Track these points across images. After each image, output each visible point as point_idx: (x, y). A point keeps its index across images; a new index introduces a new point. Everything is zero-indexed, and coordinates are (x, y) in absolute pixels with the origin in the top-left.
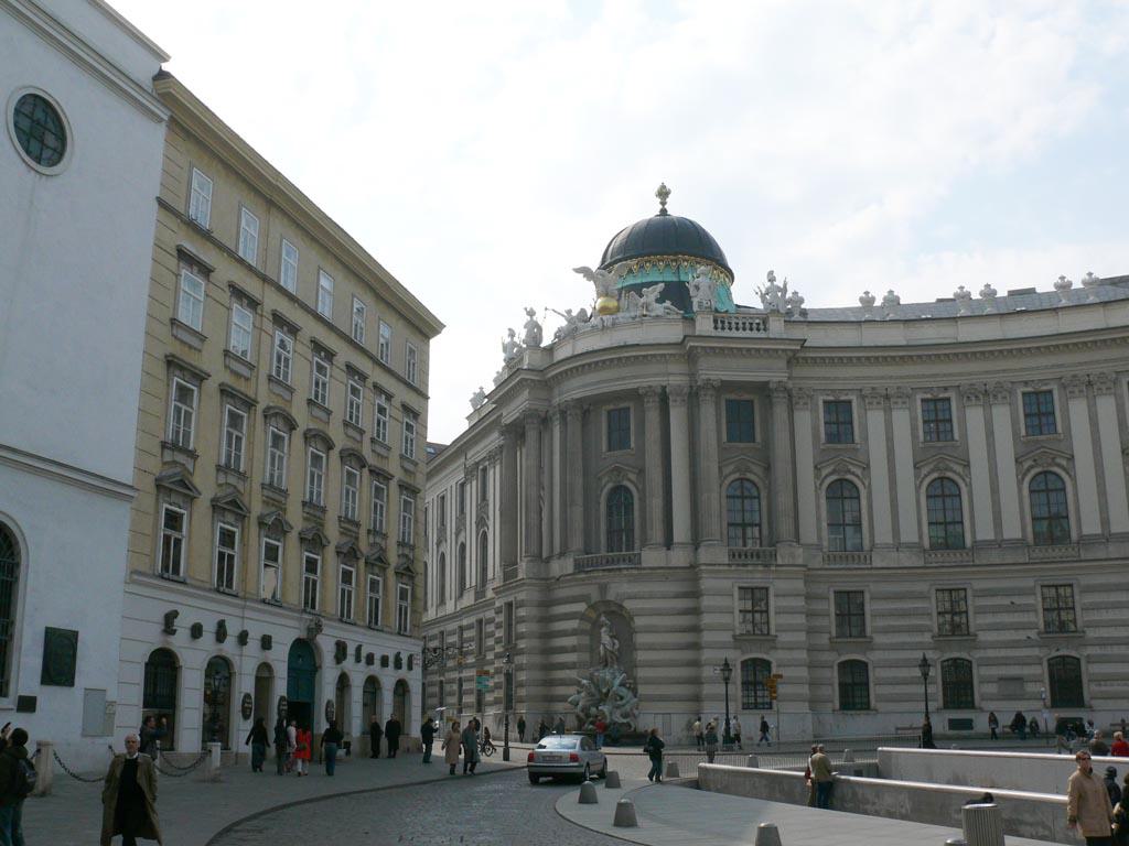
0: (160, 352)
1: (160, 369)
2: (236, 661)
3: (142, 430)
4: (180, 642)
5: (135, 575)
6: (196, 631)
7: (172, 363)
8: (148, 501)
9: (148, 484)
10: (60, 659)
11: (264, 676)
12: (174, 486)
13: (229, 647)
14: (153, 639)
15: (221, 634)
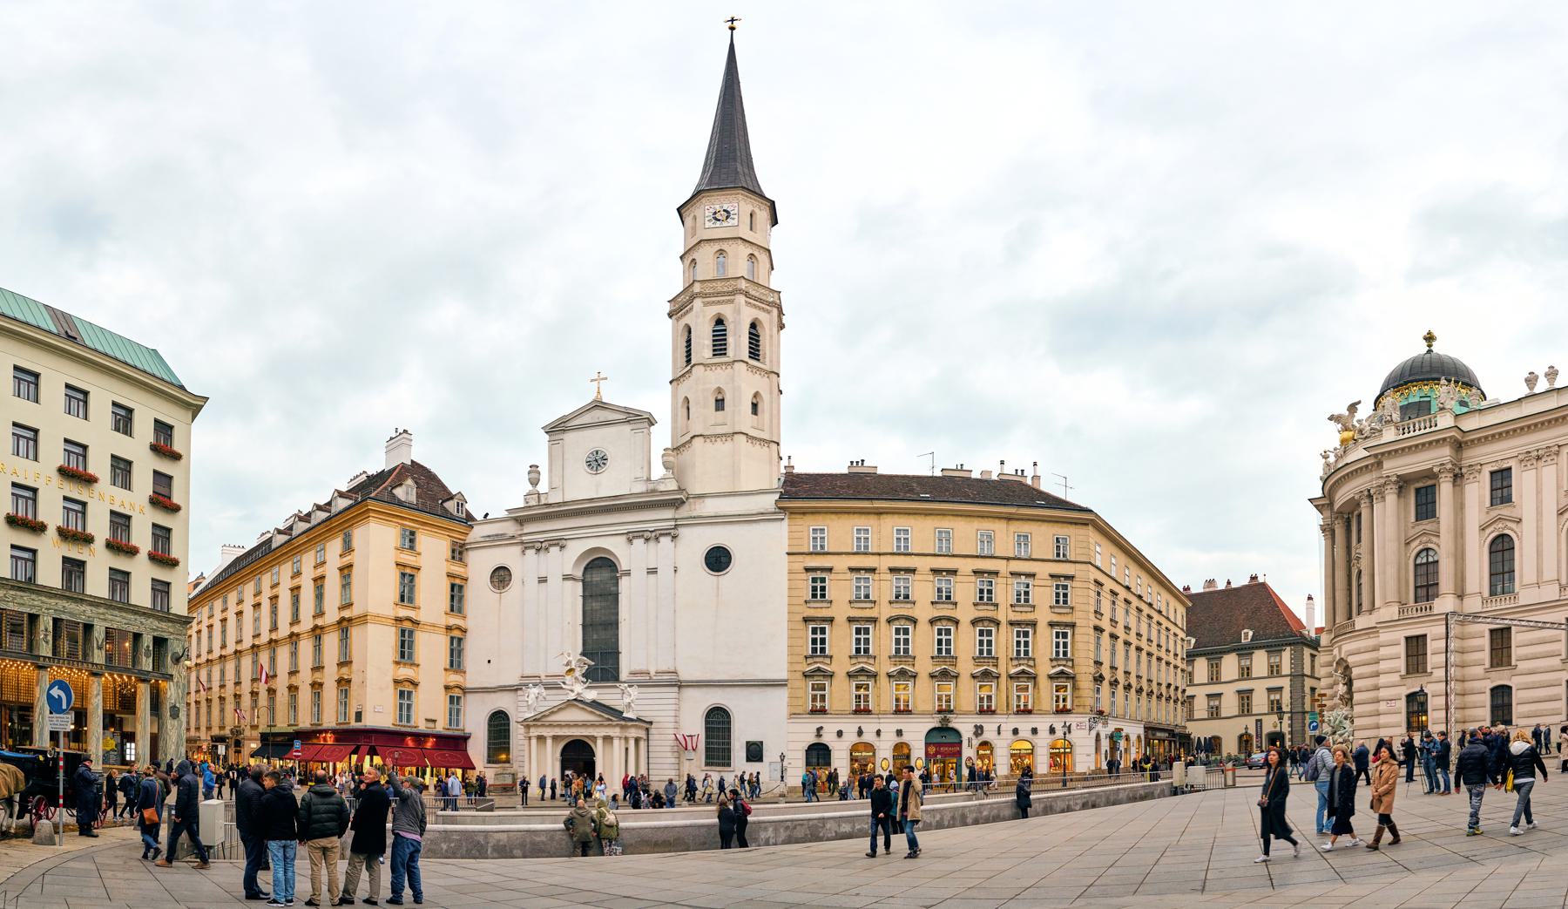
0: (800, 618)
1: (802, 625)
2: (876, 744)
3: (791, 654)
4: (828, 738)
5: (793, 715)
6: (840, 734)
7: (806, 620)
8: (800, 683)
9: (799, 675)
10: (755, 752)
11: (902, 753)
12: (818, 676)
13: (869, 737)
14: (813, 740)
15: (860, 733)
